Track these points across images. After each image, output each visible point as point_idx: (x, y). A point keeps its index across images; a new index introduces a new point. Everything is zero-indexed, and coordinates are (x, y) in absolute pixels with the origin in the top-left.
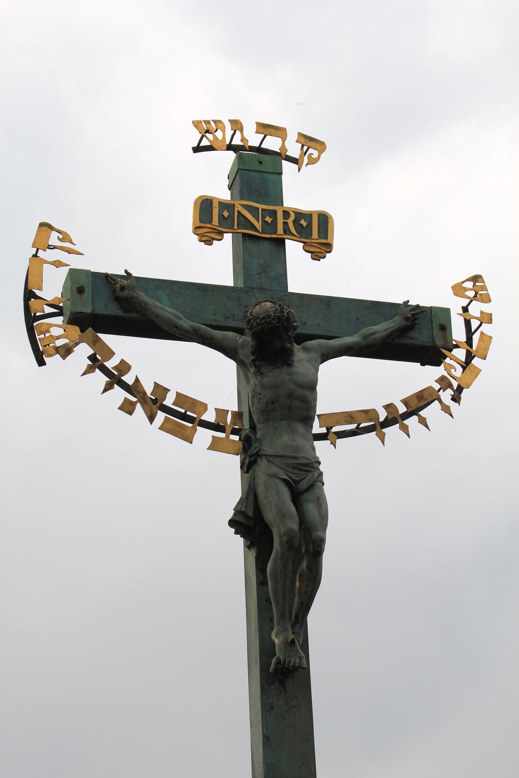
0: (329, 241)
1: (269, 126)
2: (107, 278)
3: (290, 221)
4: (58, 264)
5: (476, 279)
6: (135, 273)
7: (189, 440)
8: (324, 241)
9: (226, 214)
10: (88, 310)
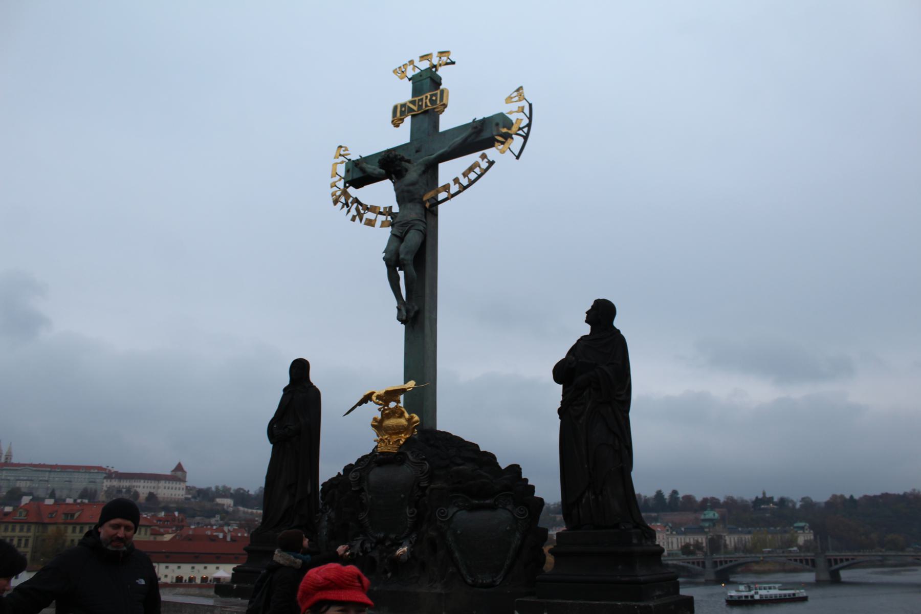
0: (444, 102)
5: (518, 90)
7: (373, 226)
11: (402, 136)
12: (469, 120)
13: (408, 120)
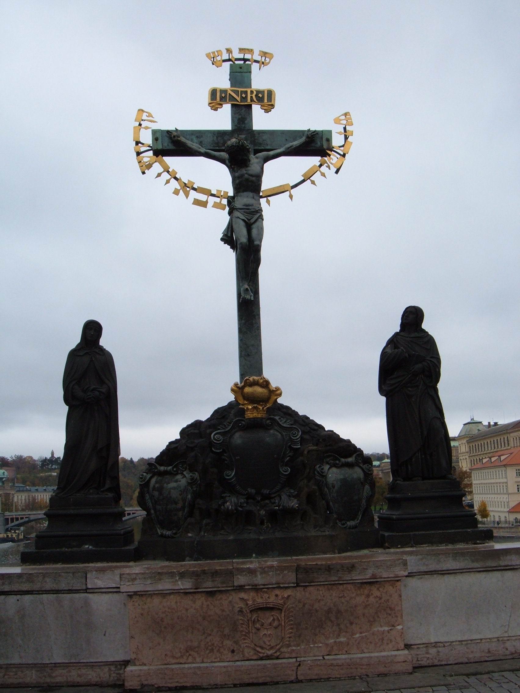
0: (272, 103)
1: (245, 49)
2: (168, 132)
3: (254, 96)
4: (146, 128)
5: (346, 114)
6: (179, 129)
8: (270, 103)
9: (223, 95)
10: (160, 147)
11: (222, 120)
12: (305, 128)
13: (227, 108)
